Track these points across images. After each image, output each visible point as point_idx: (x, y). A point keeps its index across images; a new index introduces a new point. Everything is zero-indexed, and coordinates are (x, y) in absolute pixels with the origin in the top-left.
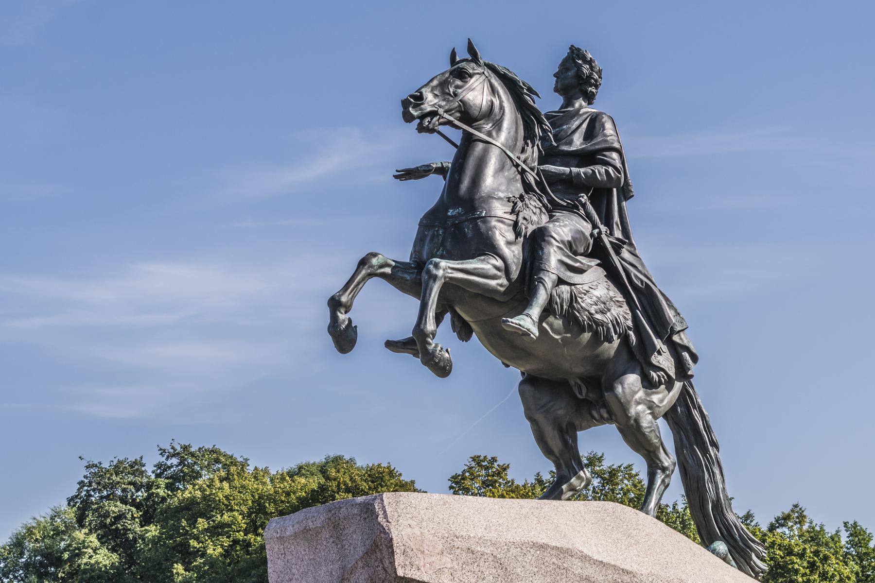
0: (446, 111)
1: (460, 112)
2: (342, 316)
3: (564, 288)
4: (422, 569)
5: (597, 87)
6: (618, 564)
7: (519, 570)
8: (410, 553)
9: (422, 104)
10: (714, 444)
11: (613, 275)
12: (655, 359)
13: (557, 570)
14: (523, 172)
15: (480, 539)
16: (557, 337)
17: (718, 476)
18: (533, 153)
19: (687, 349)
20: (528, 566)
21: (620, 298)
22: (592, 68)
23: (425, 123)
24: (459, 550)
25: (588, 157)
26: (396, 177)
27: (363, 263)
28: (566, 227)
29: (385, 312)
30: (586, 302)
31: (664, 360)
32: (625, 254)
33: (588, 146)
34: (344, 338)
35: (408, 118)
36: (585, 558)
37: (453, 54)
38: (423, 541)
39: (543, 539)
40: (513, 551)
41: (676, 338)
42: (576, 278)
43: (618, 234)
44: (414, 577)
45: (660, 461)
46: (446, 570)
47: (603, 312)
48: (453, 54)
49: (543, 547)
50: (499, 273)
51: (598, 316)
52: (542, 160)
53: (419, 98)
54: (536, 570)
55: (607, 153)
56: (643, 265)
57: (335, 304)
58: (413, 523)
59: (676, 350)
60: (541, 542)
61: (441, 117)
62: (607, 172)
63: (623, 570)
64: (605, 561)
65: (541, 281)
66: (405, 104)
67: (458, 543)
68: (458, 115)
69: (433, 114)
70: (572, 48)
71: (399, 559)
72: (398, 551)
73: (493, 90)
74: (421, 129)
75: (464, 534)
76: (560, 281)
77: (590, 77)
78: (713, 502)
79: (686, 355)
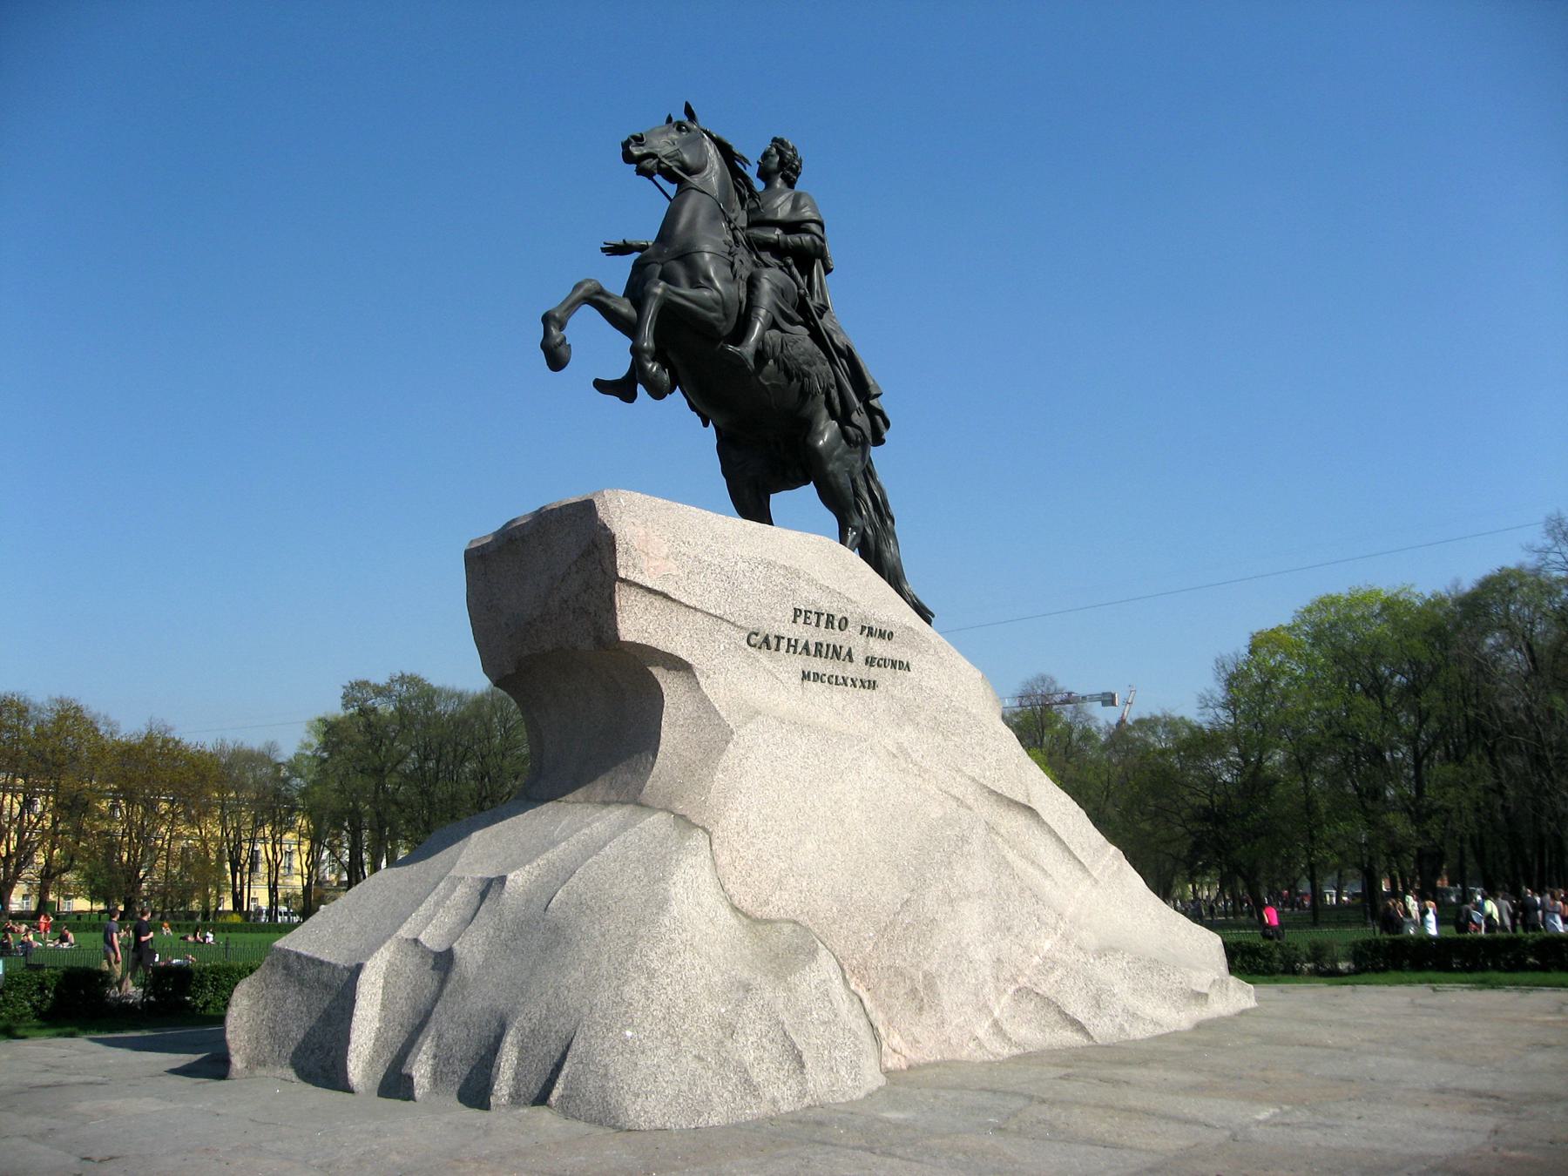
2: (554, 331)
5: (797, 174)
11: (817, 336)
12: (855, 417)
19: (881, 413)
25: (792, 227)
26: (604, 250)
27: (578, 286)
33: (795, 218)
34: (556, 358)
35: (628, 157)
41: (874, 402)
42: (787, 326)
48: (669, 120)
51: (805, 367)
52: (751, 225)
57: (547, 319)
58: (638, 522)
59: (873, 412)
61: (660, 162)
66: (626, 145)
69: (652, 156)
71: (621, 560)
74: (641, 171)
76: (774, 325)
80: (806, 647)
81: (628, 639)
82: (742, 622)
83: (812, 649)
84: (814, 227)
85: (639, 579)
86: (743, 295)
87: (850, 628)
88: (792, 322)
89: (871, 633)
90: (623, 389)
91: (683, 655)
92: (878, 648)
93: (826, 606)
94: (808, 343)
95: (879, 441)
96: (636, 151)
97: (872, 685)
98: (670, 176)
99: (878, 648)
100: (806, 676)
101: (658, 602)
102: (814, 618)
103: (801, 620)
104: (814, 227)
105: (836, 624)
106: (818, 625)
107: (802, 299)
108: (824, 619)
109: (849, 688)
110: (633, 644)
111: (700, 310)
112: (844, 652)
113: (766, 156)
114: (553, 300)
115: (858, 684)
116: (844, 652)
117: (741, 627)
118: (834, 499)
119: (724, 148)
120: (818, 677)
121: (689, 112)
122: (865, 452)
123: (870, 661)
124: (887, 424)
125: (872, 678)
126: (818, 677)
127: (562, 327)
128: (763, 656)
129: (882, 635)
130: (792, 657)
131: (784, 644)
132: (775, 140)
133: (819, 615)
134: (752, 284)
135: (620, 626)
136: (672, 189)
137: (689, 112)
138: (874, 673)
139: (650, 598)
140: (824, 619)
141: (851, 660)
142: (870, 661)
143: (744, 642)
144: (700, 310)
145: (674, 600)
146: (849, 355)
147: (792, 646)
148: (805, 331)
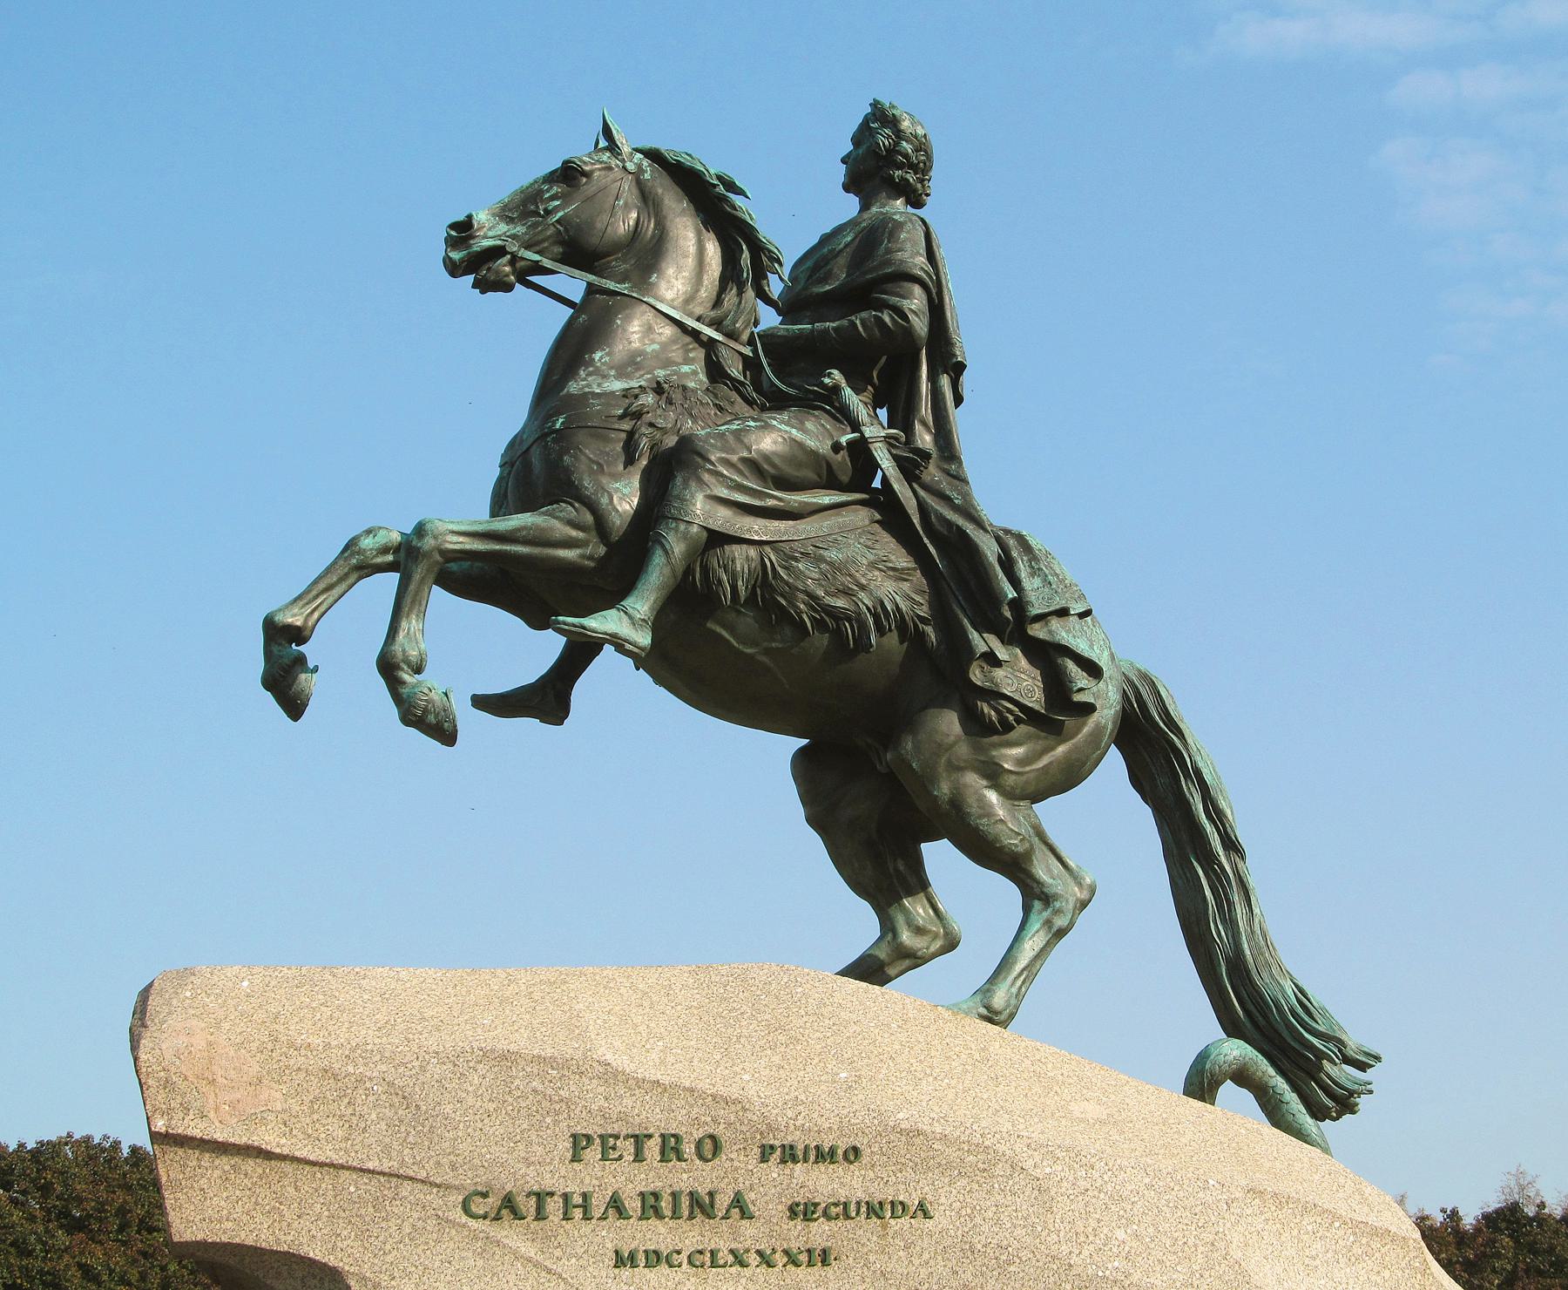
0: (528, 246)
1: (561, 243)
3: (738, 552)
4: (212, 1115)
5: (923, 169)
6: (704, 1085)
7: (448, 1109)
8: (182, 1085)
9: (474, 237)
10: (1231, 845)
13: (545, 1104)
15: (353, 1050)
16: (749, 651)
17: (1240, 911)
20: (470, 1100)
21: (902, 560)
22: (899, 134)
24: (302, 1075)
31: (1019, 680)
32: (932, 473)
35: (454, 269)
36: (611, 1075)
38: (211, 1060)
39: (520, 1042)
40: (435, 1070)
41: (1037, 631)
43: (925, 439)
44: (190, 1132)
45: (1038, 882)
46: (271, 1117)
47: (846, 593)
49: (506, 1059)
50: (581, 535)
53: (463, 230)
54: (492, 1106)
55: (889, 286)
56: (966, 496)
60: (502, 1045)
61: (514, 259)
62: (879, 321)
63: (714, 1097)
64: (666, 1080)
65: (659, 541)
67: (297, 1060)
68: (558, 249)
69: (498, 252)
70: (875, 105)
72: (150, 1082)
73: (646, 197)
74: (483, 286)
75: (316, 1041)
77: (893, 151)
78: (1228, 961)
79: (1071, 665)
80: (616, 1205)
81: (188, 1236)
82: (449, 1177)
83: (633, 1205)
85: (196, 1130)
87: (730, 1153)
89: (790, 1155)
91: (316, 1252)
92: (823, 1182)
93: (655, 1118)
96: (456, 256)
97: (825, 1257)
99: (823, 1182)
100: (623, 1260)
101: (250, 1165)
102: (629, 1146)
103: (593, 1153)
105: (688, 1149)
106: (639, 1157)
107: (860, 449)
108: (652, 1148)
109: (755, 1269)
110: (203, 1245)
111: (536, 551)
112: (722, 1202)
115: (780, 1259)
116: (722, 1202)
117: (448, 1187)
119: (688, 179)
120: (655, 1258)
123: (803, 1211)
125: (818, 1243)
126: (655, 1258)
127: (299, 635)
128: (510, 1234)
129: (825, 1156)
130: (579, 1229)
131: (554, 1206)
133: (639, 1140)
135: (173, 1217)
138: (820, 1232)
139: (225, 1162)
140: (652, 1148)
141: (745, 1214)
142: (803, 1211)
143: (458, 1215)
144: (536, 551)
145: (283, 1158)
146: (960, 548)
147: (578, 1206)
148: (862, 517)
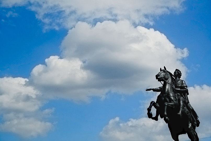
14: (173, 89)
18: (174, 86)
23: (160, 80)
27: (151, 103)
28: (181, 98)
29: (154, 111)
30: (186, 112)
31: (195, 123)
35: (157, 78)
37: (161, 69)
48: (161, 69)
70: (176, 70)
84: (186, 87)
86: (178, 103)
88: (184, 106)
90: (156, 119)
94: (187, 110)
95: (198, 126)
98: (163, 80)
104: (186, 87)
113: (175, 73)
114: (148, 106)
118: (190, 136)
121: (165, 68)
122: (195, 128)
124: (199, 123)
127: (150, 110)
132: (176, 70)
134: (179, 100)
136: (163, 82)
137: (165, 68)
